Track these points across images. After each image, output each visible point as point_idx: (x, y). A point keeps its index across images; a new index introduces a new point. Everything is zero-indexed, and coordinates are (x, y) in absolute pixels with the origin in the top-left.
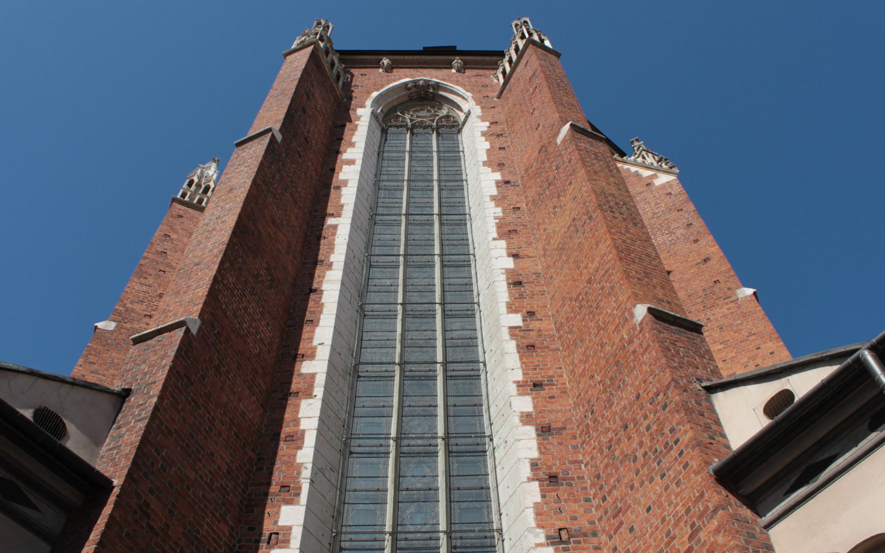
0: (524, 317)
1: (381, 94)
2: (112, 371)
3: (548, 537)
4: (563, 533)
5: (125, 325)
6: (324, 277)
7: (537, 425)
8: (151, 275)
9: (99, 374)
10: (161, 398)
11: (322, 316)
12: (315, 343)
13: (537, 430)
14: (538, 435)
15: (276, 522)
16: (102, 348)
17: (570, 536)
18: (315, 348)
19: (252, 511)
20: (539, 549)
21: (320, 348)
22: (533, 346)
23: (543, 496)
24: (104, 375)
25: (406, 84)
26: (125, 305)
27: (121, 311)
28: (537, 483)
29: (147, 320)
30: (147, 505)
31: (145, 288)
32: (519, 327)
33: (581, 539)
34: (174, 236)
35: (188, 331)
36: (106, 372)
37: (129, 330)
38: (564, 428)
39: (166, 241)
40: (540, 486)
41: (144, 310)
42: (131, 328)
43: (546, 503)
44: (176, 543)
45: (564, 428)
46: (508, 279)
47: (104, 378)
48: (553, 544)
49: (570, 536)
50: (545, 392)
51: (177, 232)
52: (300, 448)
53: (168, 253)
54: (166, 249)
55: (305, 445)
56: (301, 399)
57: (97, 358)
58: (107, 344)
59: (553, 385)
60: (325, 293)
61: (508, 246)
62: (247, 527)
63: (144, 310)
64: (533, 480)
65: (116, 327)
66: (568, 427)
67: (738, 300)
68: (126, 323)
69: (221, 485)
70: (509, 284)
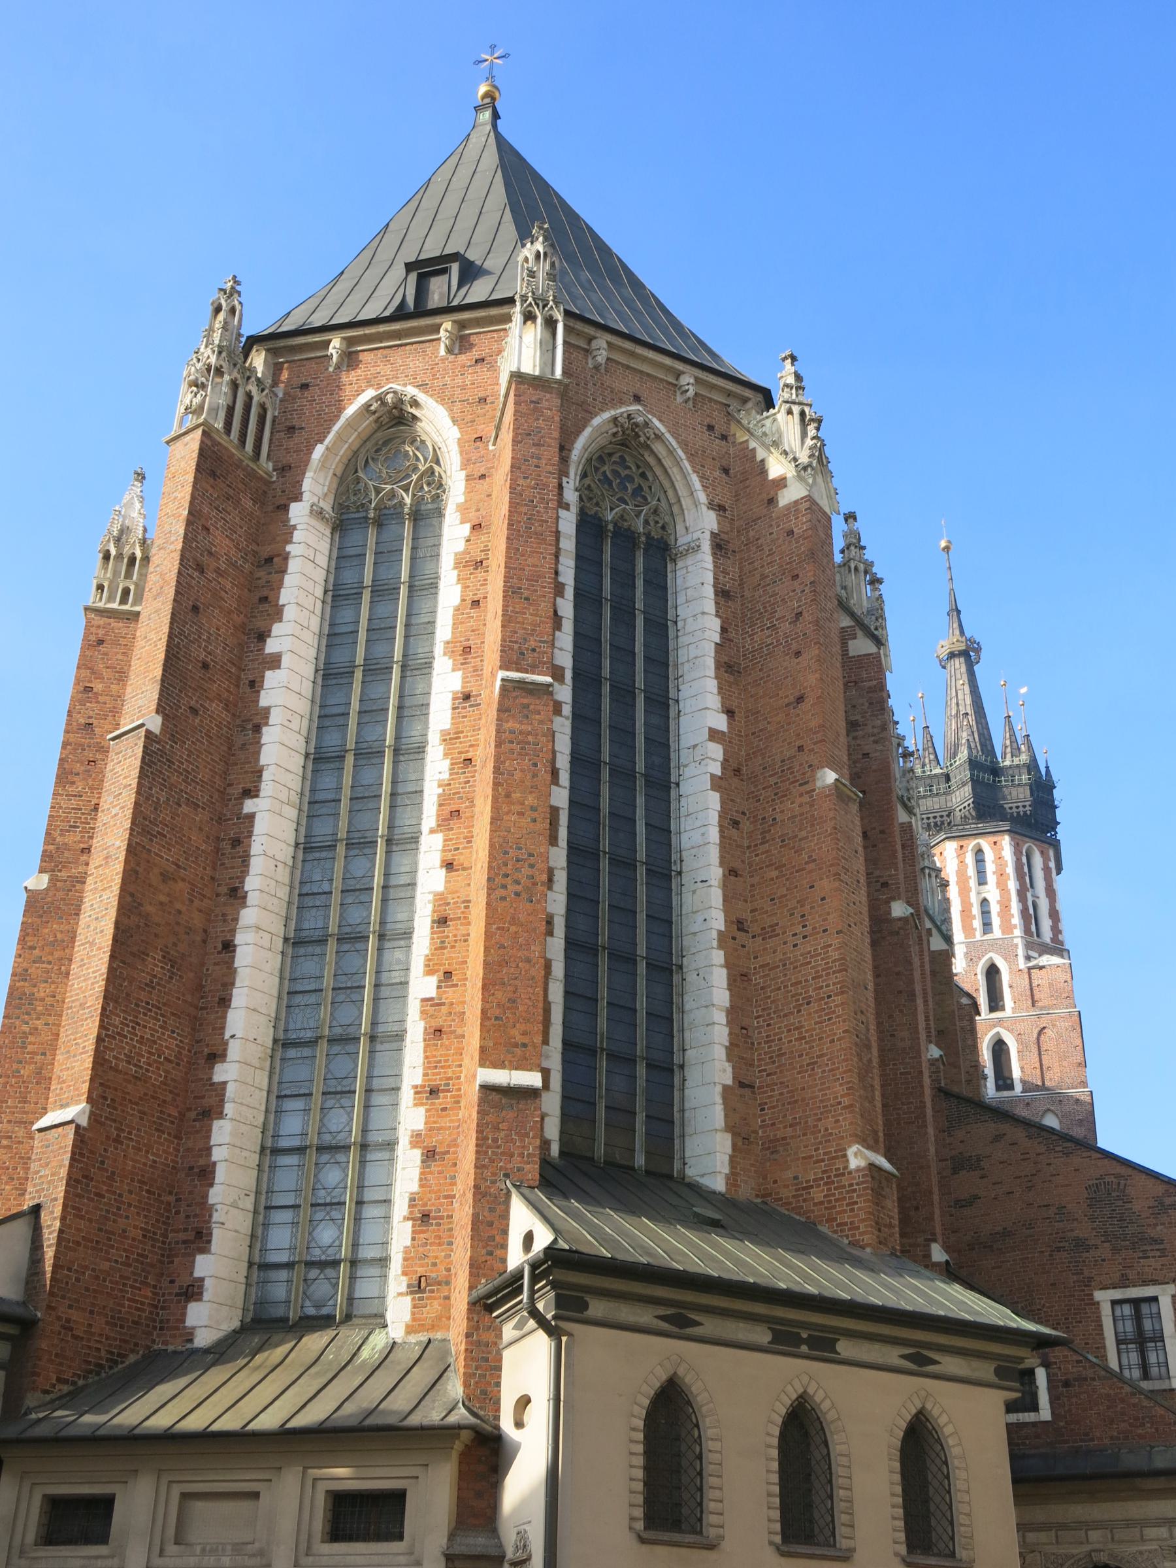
0: (440, 981)
1: (338, 417)
2: (57, 954)
3: (409, 1286)
4: (423, 1279)
5: (59, 874)
6: (236, 920)
7: (424, 1148)
8: (78, 774)
9: (44, 963)
10: (63, 1219)
11: (235, 991)
12: (227, 1037)
13: (423, 1154)
14: (423, 1162)
15: (192, 1273)
16: (38, 920)
17: (428, 1285)
18: (226, 1044)
19: (172, 1262)
20: (400, 1298)
21: (232, 1043)
22: (440, 1031)
23: (413, 1239)
24: (49, 963)
25: (367, 406)
26: (54, 839)
27: (51, 852)
28: (410, 1223)
29: (84, 858)
30: (68, 1320)
31: (74, 802)
32: (431, 999)
33: (435, 1288)
34: (98, 687)
35: (78, 1127)
36: (50, 958)
37: (66, 881)
38: (448, 1152)
39: (89, 699)
40: (413, 1226)
41: (80, 842)
42: (68, 877)
43: (414, 1247)
44: (101, 1335)
45: (448, 1152)
46: (434, 911)
47: (50, 967)
48: (412, 1293)
49: (428, 1285)
50: (439, 1102)
51: (100, 677)
52: (211, 1185)
53: (95, 722)
54: (91, 717)
55: (217, 1181)
56: (212, 1120)
57: (36, 939)
58: (45, 912)
59: (448, 1091)
60: (238, 949)
61: (444, 846)
62: (169, 1279)
63: (80, 842)
64: (408, 1219)
65: (50, 880)
66: (452, 1150)
67: (814, 790)
68: (60, 871)
69: (138, 1254)
70: (433, 922)
